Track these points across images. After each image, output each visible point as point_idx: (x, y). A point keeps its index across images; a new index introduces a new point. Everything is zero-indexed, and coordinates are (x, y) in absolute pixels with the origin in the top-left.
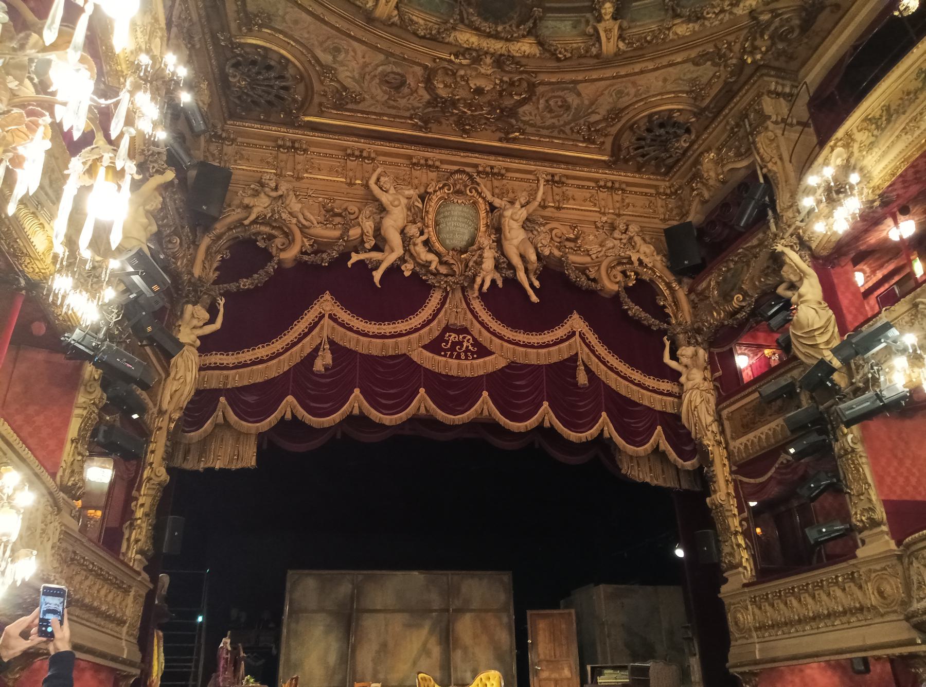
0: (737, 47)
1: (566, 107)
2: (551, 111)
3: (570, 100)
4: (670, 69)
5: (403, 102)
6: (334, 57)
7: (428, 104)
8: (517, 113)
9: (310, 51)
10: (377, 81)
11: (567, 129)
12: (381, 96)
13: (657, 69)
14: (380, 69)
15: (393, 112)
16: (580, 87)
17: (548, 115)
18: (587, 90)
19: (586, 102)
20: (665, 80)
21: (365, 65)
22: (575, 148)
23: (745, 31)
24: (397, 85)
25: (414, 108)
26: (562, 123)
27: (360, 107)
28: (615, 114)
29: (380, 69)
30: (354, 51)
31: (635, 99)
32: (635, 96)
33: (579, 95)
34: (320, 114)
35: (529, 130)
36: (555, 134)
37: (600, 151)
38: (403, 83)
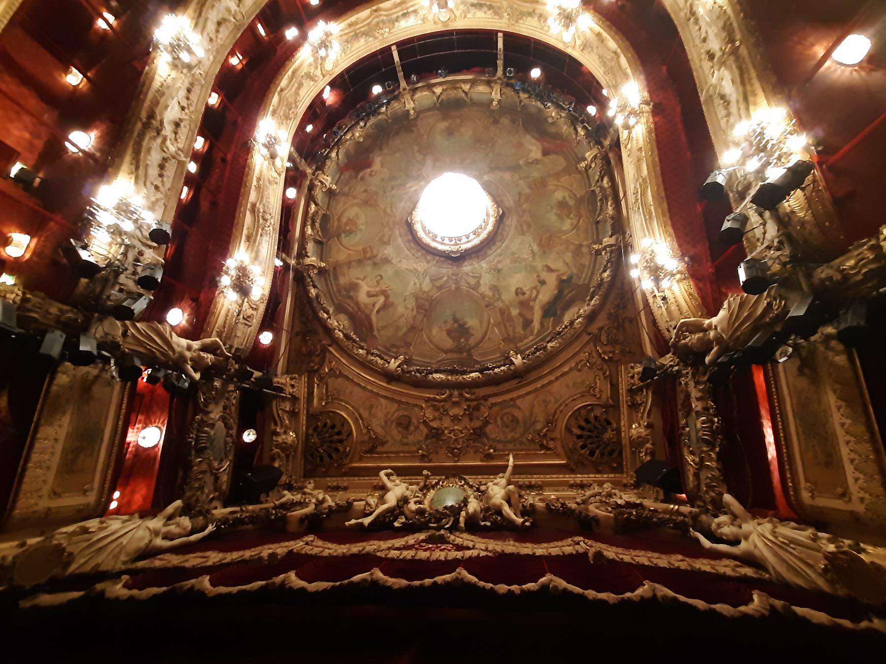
0: (595, 355)
1: (515, 420)
2: (507, 427)
3: (515, 414)
4: (566, 377)
5: (411, 438)
6: (370, 411)
7: (427, 437)
8: (485, 434)
9: (357, 411)
10: (394, 424)
11: (524, 440)
12: (398, 437)
13: (557, 379)
14: (396, 415)
15: (405, 448)
16: (518, 402)
17: (507, 430)
18: (523, 404)
19: (527, 414)
20: (567, 386)
21: (387, 414)
22: (536, 456)
23: (592, 344)
24: (405, 425)
25: (419, 442)
26: (518, 435)
27: (386, 448)
28: (550, 422)
29: (396, 415)
30: (381, 405)
31: (556, 406)
32: (556, 401)
33: (520, 408)
34: (361, 459)
35: (499, 446)
36: (518, 446)
37: (557, 456)
38: (410, 423)
